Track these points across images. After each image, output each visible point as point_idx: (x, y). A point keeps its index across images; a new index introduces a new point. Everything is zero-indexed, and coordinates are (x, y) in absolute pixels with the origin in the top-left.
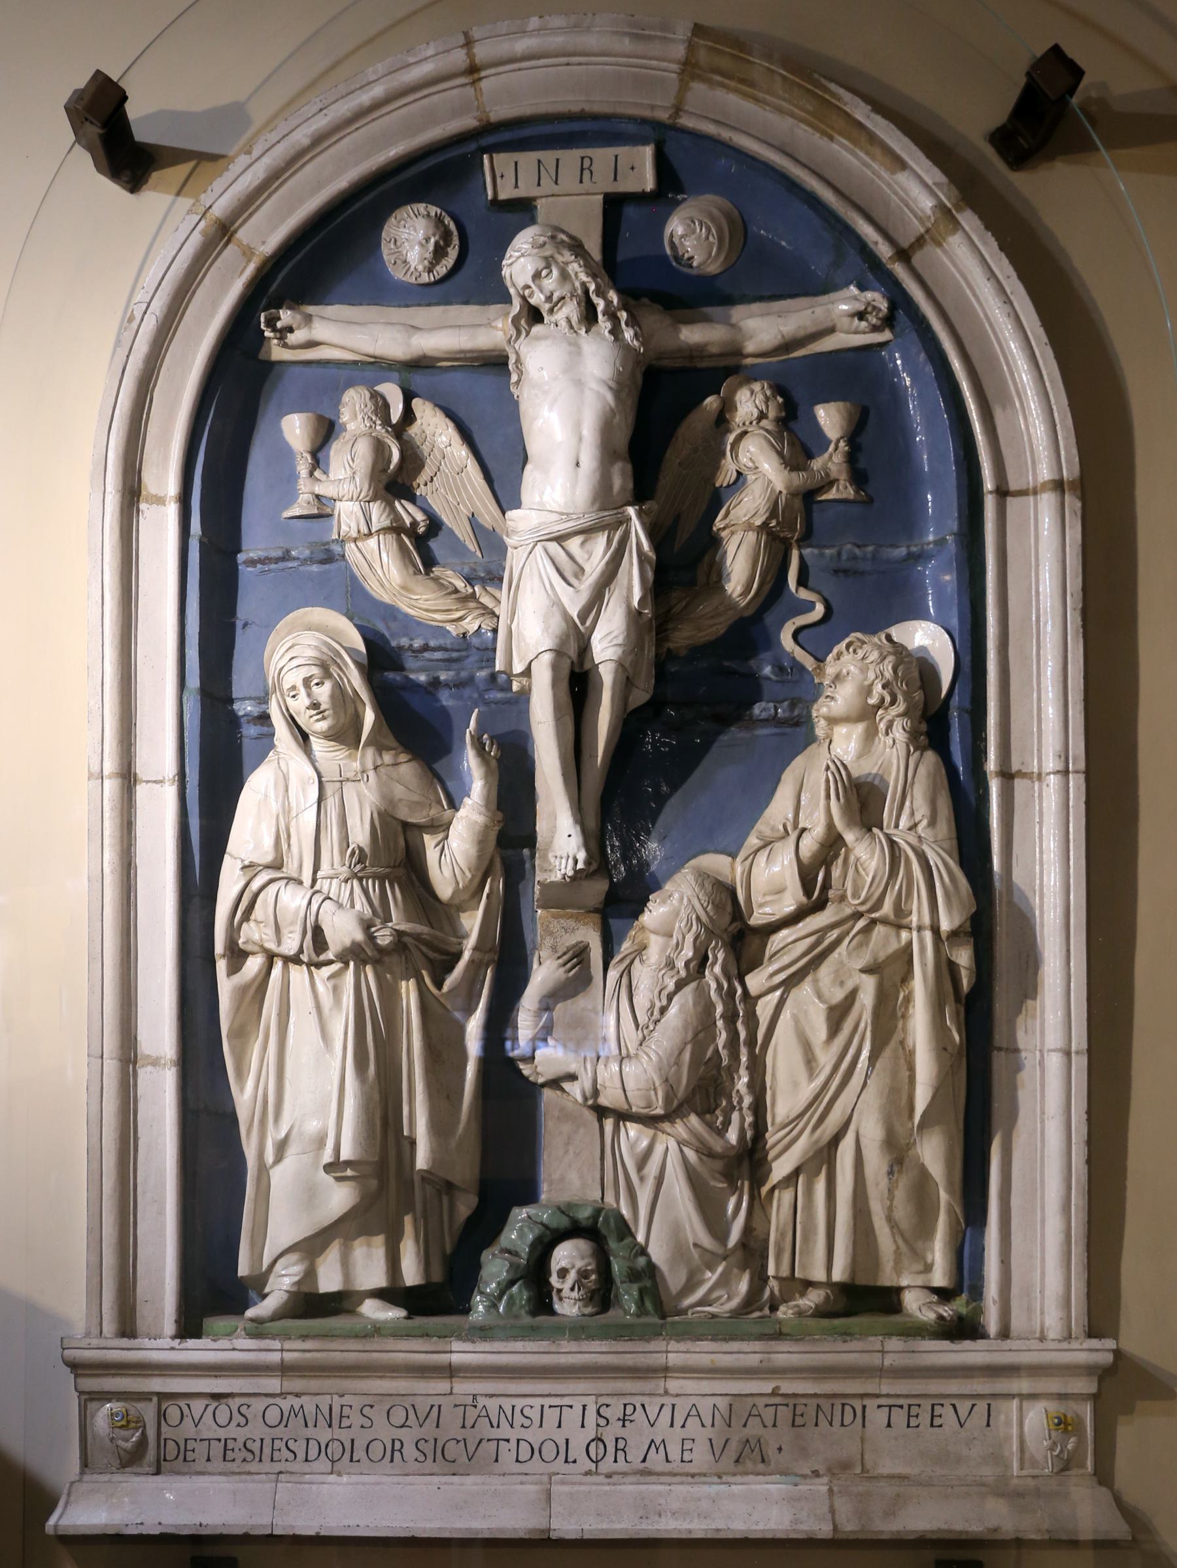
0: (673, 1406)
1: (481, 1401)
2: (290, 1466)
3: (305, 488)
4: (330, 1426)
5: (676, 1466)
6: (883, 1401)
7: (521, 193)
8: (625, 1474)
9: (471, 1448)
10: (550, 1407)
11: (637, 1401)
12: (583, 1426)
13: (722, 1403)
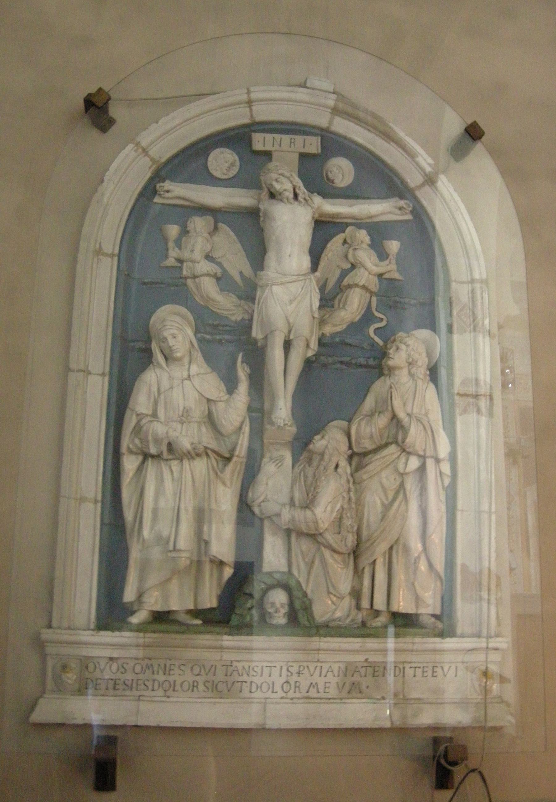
0: (321, 667)
1: (235, 664)
2: (145, 693)
3: (174, 253)
4: (165, 674)
5: (322, 695)
6: (413, 665)
7: (268, 148)
8: (299, 698)
9: (229, 686)
10: (267, 667)
11: (305, 664)
12: (281, 676)
13: (343, 666)
